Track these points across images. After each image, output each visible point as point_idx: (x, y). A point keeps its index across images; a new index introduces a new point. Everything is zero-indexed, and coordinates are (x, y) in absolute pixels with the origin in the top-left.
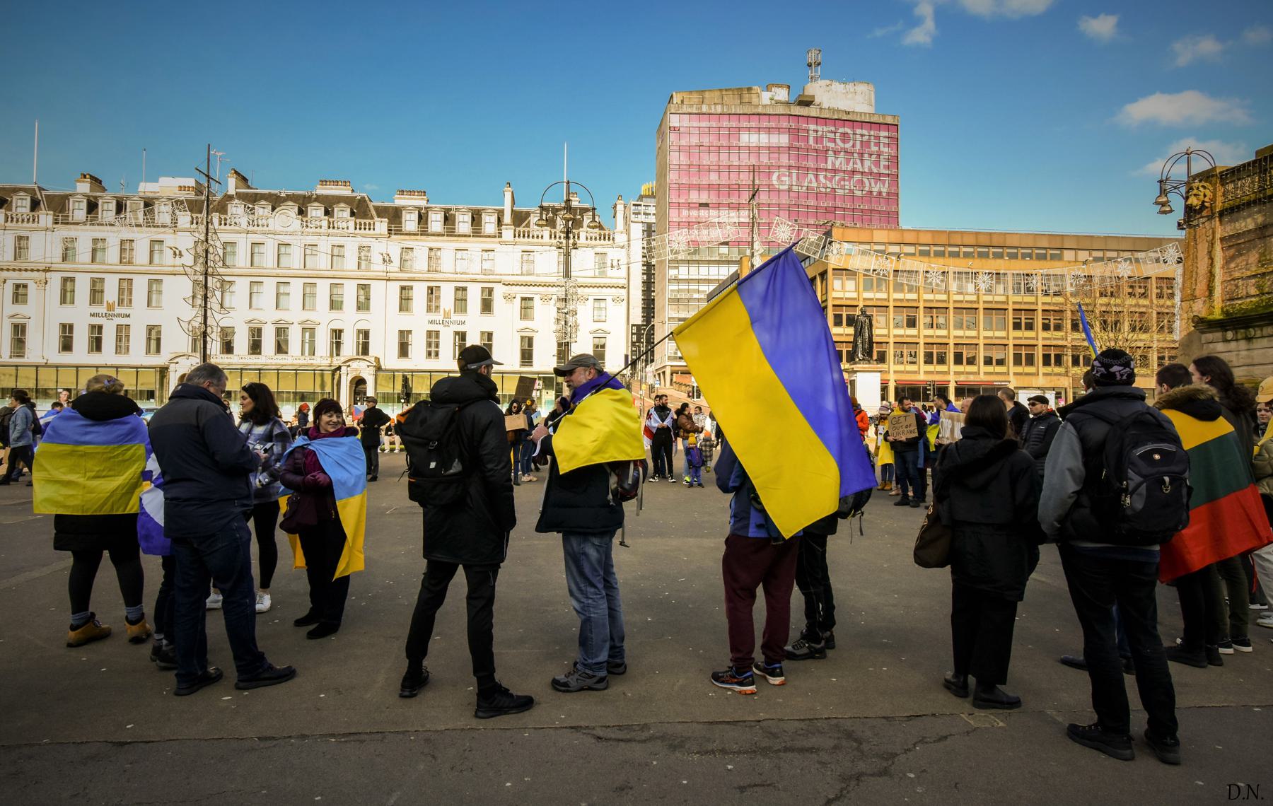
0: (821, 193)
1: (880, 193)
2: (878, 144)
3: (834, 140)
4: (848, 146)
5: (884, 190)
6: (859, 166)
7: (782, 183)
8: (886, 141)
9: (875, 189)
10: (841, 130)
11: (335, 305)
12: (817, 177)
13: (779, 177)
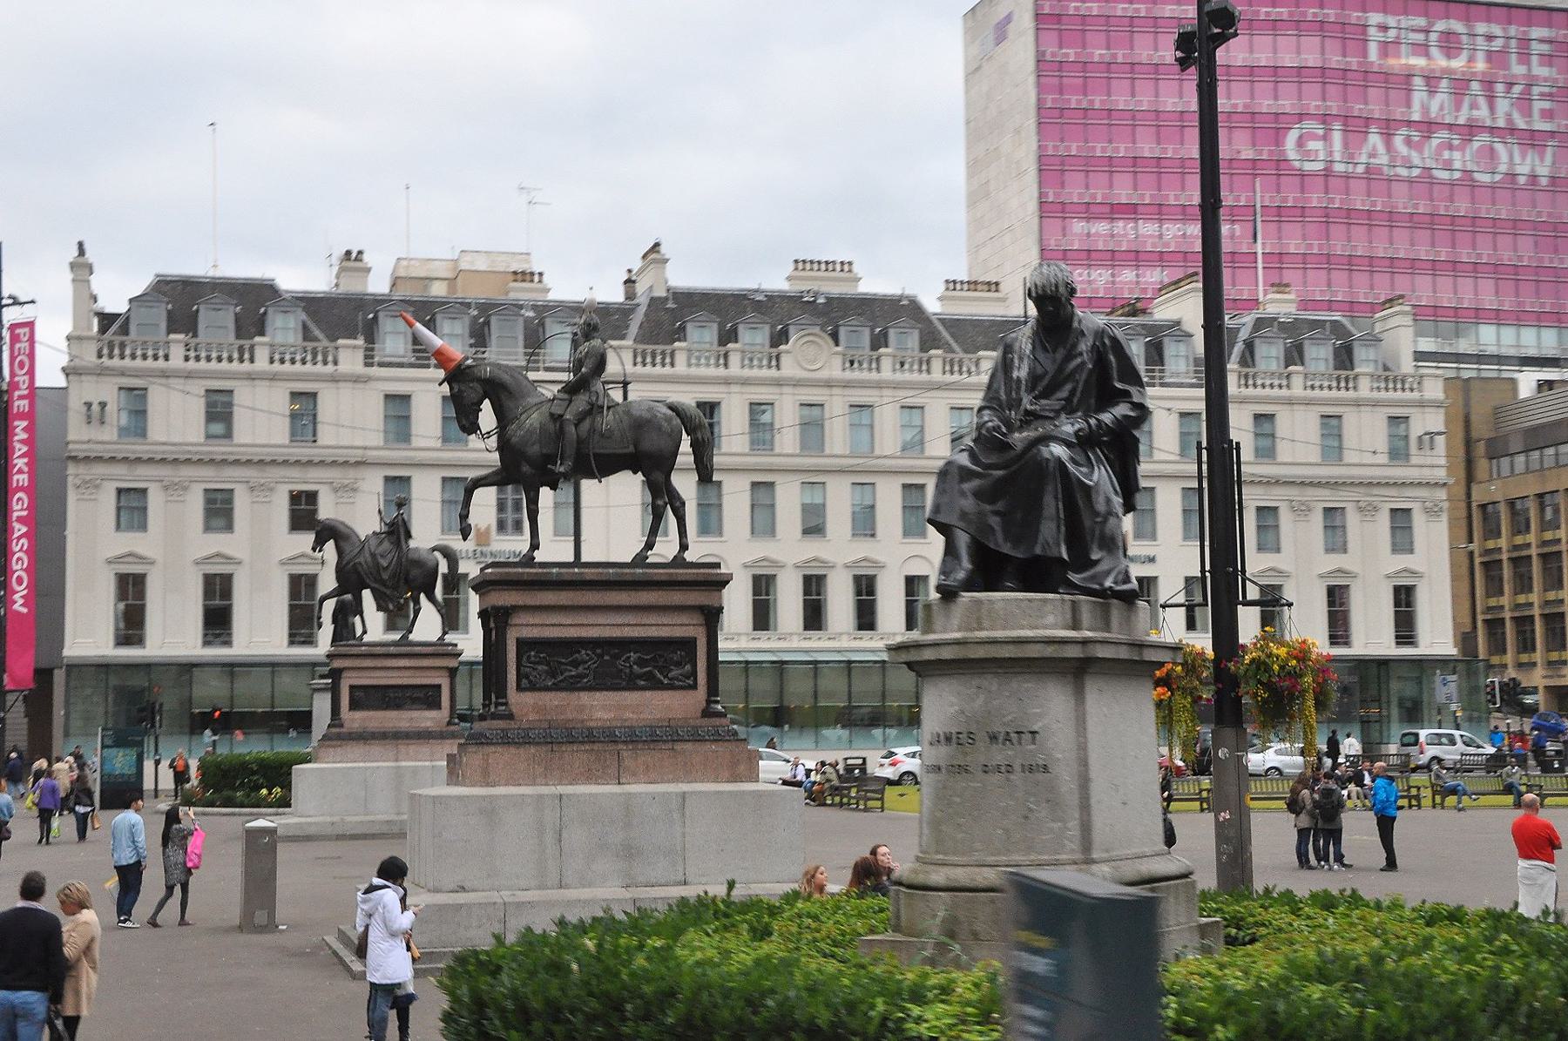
1: (1533, 178)
2: (1524, 57)
3: (1422, 49)
4: (1458, 63)
5: (1543, 171)
6: (1482, 113)
7: (1308, 156)
8: (1545, 48)
9: (1523, 169)
10: (1440, 26)
11: (814, 527)
12: (1388, 137)
13: (1300, 143)
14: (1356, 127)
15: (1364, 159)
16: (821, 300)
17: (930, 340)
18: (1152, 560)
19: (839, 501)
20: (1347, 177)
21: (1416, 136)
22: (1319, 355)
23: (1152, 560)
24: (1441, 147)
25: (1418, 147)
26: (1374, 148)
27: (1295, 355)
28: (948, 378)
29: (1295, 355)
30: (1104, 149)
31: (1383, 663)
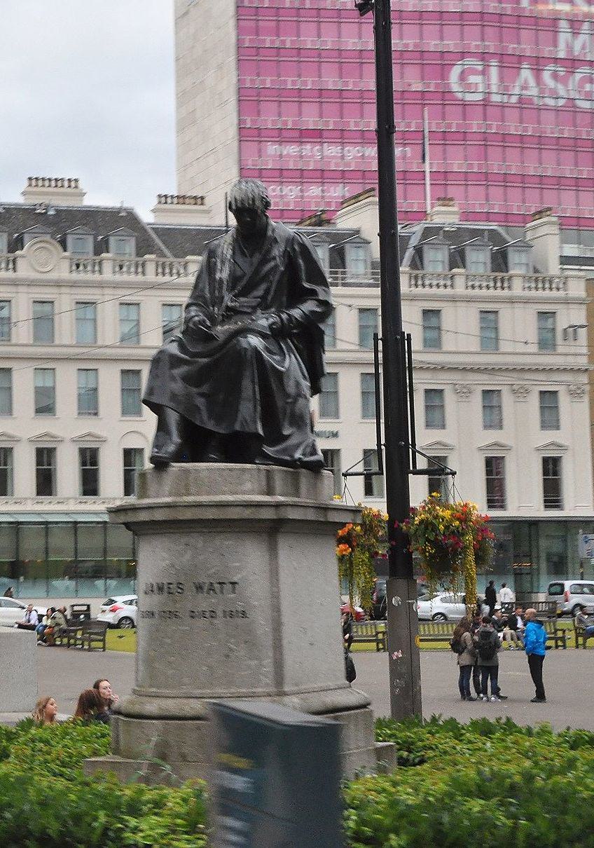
0: (547, 108)
7: (469, 88)
11: (45, 407)
12: (537, 72)
13: (463, 76)
14: (510, 63)
15: (517, 91)
16: (51, 212)
17: (145, 246)
18: (335, 435)
19: (67, 384)
20: (502, 106)
21: (562, 71)
22: (479, 259)
23: (335, 435)
24: (583, 81)
25: (564, 81)
26: (526, 81)
27: (458, 259)
28: (161, 279)
29: (458, 259)
30: (294, 83)
31: (534, 524)
